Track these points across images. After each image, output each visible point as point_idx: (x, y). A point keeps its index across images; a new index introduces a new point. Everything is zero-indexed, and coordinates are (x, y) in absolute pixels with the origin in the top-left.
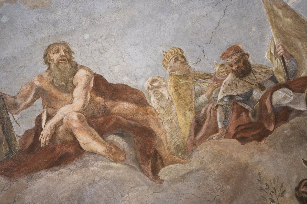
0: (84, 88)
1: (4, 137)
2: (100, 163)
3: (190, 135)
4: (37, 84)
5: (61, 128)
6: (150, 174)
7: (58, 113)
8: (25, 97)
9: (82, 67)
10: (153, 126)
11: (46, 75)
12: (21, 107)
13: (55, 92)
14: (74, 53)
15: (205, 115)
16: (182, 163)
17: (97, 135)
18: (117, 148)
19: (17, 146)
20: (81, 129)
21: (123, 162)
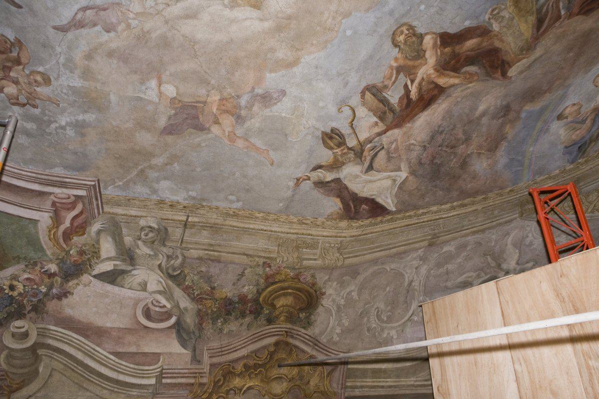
0: (433, 48)
1: (387, 108)
2: (459, 90)
3: (533, 34)
4: (395, 65)
5: (424, 83)
6: (500, 77)
7: (419, 75)
8: (390, 78)
9: (427, 34)
10: (497, 44)
11: (399, 56)
12: (390, 86)
13: (411, 63)
14: (415, 27)
15: (547, 11)
16: (527, 58)
17: (452, 74)
18: (471, 74)
19: (397, 108)
20: (439, 76)
21: (477, 80)
